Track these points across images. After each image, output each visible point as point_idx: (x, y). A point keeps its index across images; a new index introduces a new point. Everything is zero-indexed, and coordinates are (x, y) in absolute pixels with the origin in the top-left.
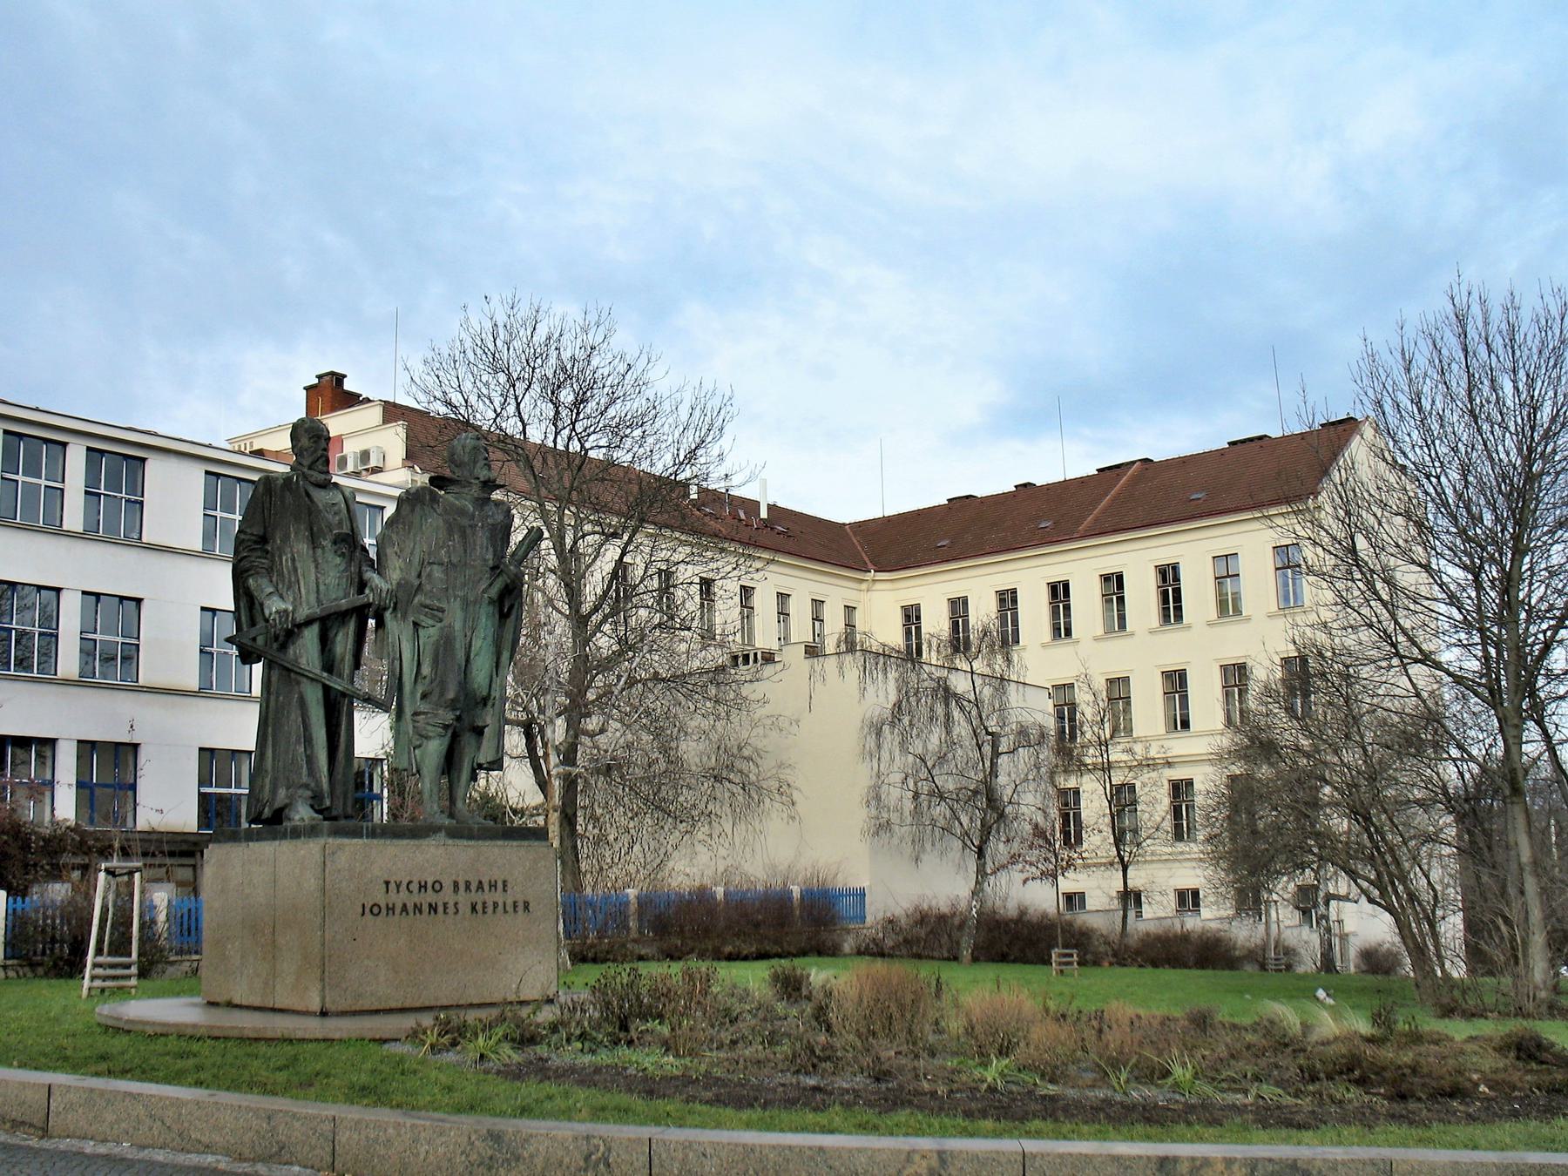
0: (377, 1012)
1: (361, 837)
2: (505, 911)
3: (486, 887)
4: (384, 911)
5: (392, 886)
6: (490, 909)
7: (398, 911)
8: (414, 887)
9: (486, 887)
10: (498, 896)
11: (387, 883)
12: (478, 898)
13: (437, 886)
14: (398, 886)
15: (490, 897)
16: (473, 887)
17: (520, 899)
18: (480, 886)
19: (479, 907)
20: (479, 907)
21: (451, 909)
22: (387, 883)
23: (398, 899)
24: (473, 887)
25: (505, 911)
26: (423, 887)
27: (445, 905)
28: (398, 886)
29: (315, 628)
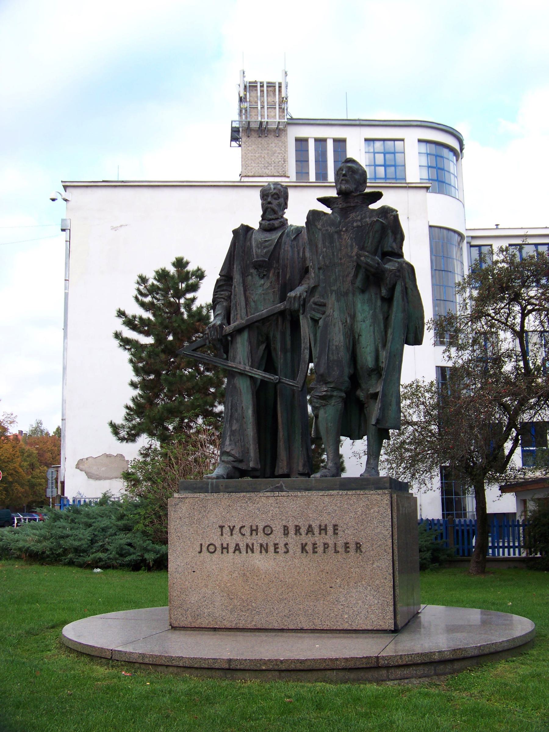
0: (215, 629)
1: (207, 492)
2: (336, 552)
3: (316, 531)
4: (219, 549)
5: (226, 530)
6: (320, 549)
7: (231, 550)
8: (247, 531)
9: (316, 531)
10: (329, 539)
11: (222, 527)
12: (309, 540)
13: (268, 531)
14: (232, 530)
15: (319, 539)
16: (303, 530)
17: (351, 540)
18: (310, 530)
19: (309, 548)
20: (309, 548)
21: (282, 549)
22: (222, 527)
23: (231, 540)
24: (303, 530)
25: (336, 552)
26: (254, 530)
27: (276, 546)
28: (232, 530)
29: (245, 335)
